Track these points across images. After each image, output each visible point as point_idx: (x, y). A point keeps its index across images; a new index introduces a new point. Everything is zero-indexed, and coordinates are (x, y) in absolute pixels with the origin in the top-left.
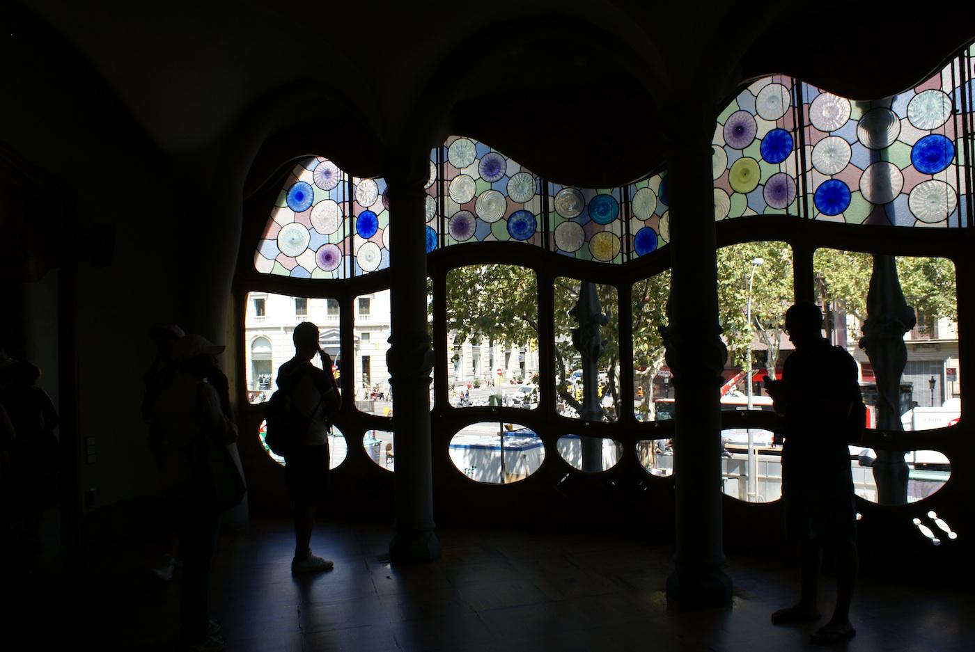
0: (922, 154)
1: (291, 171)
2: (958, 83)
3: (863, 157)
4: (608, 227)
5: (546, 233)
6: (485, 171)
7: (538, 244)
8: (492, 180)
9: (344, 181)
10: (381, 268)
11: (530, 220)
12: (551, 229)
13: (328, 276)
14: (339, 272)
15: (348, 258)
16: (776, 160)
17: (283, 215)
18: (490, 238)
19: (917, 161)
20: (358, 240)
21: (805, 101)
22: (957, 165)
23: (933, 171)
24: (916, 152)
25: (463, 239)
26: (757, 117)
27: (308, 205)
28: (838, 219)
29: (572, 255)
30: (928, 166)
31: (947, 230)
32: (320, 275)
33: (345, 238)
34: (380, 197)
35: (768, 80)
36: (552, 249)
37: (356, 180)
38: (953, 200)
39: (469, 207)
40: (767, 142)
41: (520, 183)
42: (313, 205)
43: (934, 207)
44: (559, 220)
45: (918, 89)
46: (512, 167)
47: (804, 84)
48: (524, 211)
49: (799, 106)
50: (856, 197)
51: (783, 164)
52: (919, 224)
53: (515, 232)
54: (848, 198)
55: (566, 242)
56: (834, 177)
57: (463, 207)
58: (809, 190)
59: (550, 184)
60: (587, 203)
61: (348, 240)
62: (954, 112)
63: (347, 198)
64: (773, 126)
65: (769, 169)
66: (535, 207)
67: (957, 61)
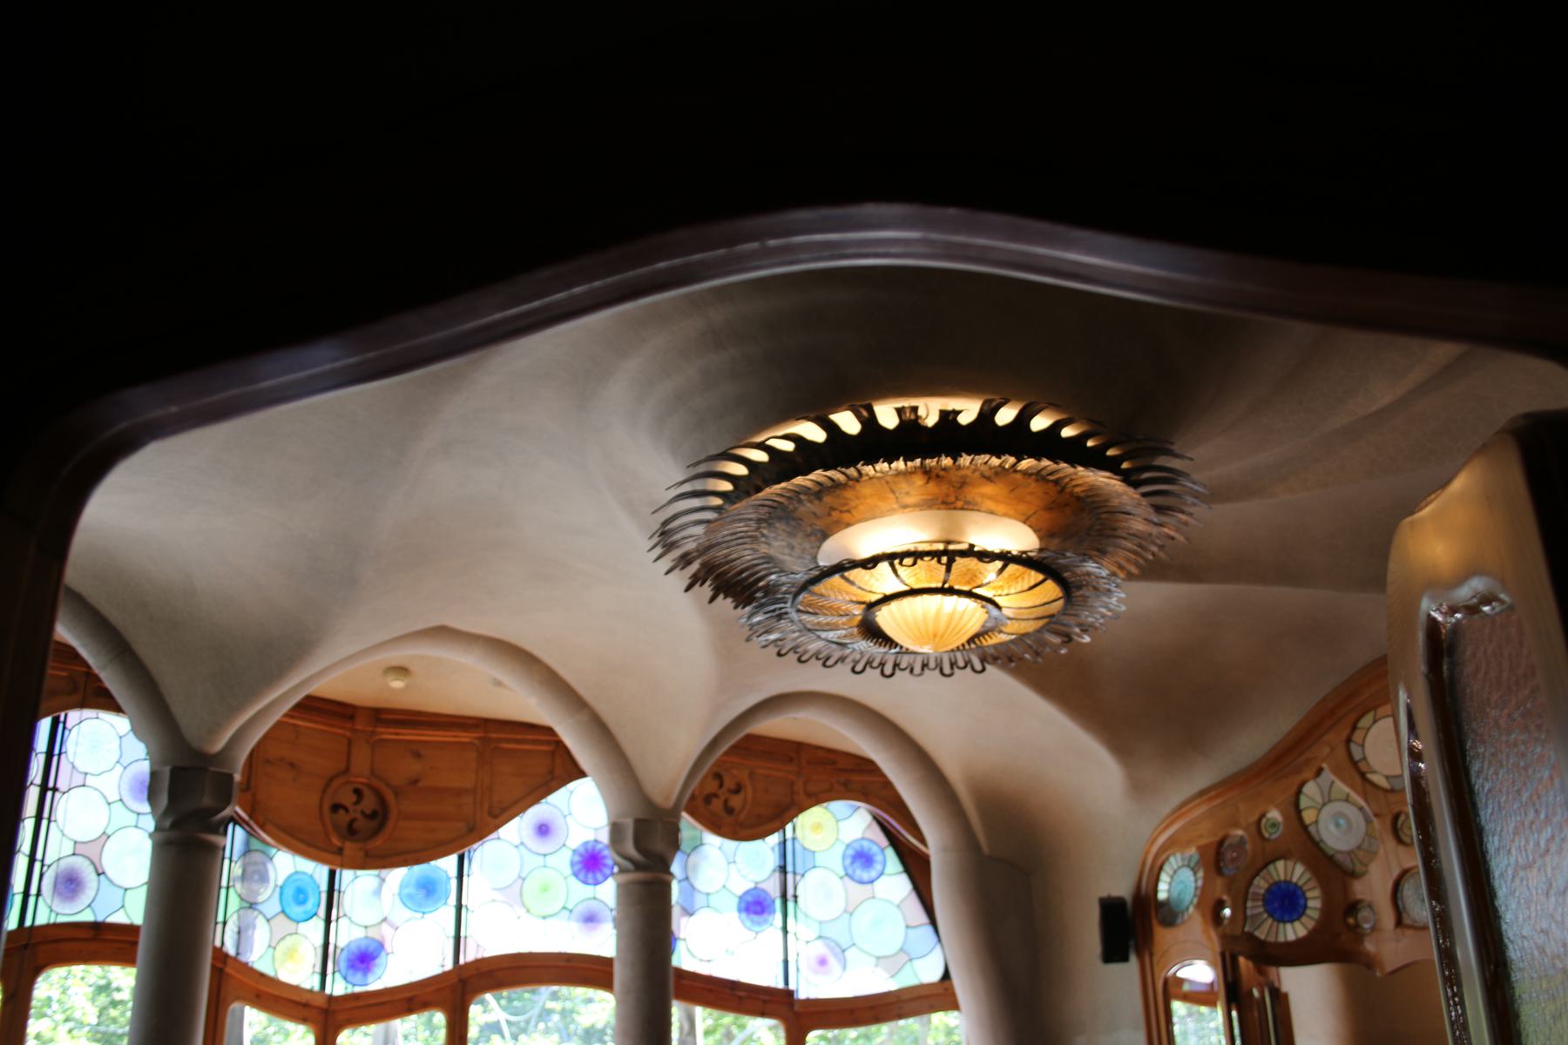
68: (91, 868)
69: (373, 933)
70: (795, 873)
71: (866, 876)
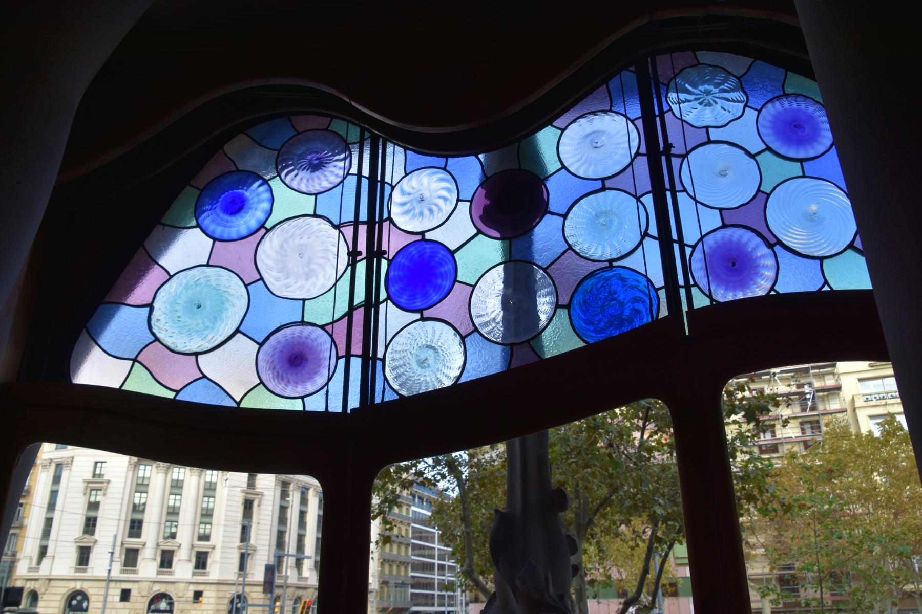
8: (802, 155)
9: (359, 175)
20: (392, 317)
27: (253, 224)
33: (352, 308)
34: (464, 207)
39: (751, 216)
42: (268, 225)
57: (729, 218)
63: (363, 216)
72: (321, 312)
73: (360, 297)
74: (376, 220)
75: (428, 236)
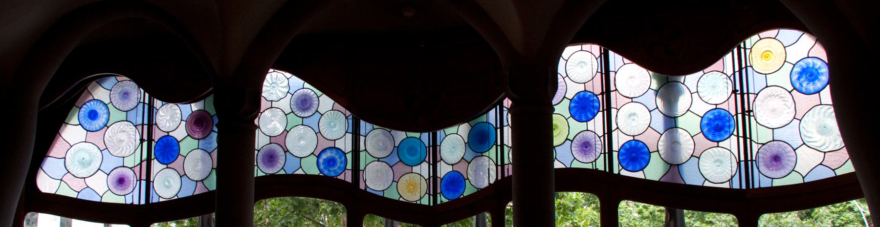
0: (708, 124)
1: (86, 88)
2: (737, 69)
3: (659, 122)
4: (416, 169)
5: (356, 170)
6: (297, 104)
7: (349, 179)
9: (144, 103)
10: (181, 196)
11: (340, 158)
12: (362, 168)
13: (120, 200)
14: (132, 196)
15: (144, 183)
16: (584, 119)
17: (72, 132)
18: (300, 172)
19: (705, 130)
20: (156, 166)
21: (612, 68)
22: (738, 136)
23: (718, 139)
24: (705, 122)
25: (271, 171)
26: (567, 79)
27: (101, 124)
28: (639, 175)
29: (381, 194)
30: (714, 135)
31: (731, 190)
32: (110, 198)
33: (142, 161)
34: (183, 123)
35: (578, 47)
36: (362, 187)
37: (158, 103)
38: (735, 165)
40: (576, 102)
41: (332, 120)
43: (719, 170)
44: (370, 159)
45: (706, 70)
46: (326, 103)
47: (611, 53)
48: (335, 147)
49: (606, 72)
50: (654, 157)
51: (591, 124)
52: (707, 184)
53: (325, 168)
54: (647, 158)
55: (376, 179)
56: (636, 138)
58: (615, 147)
59: (362, 123)
60: (397, 145)
61: (144, 164)
62: (734, 91)
63: (146, 122)
64: (581, 88)
65: (577, 127)
66: (346, 144)
67: (735, 50)
68: (281, 149)
69: (456, 168)
70: (748, 93)
71: (811, 87)
72: (130, 162)
73: (145, 156)
74: (151, 124)
75: (171, 134)
